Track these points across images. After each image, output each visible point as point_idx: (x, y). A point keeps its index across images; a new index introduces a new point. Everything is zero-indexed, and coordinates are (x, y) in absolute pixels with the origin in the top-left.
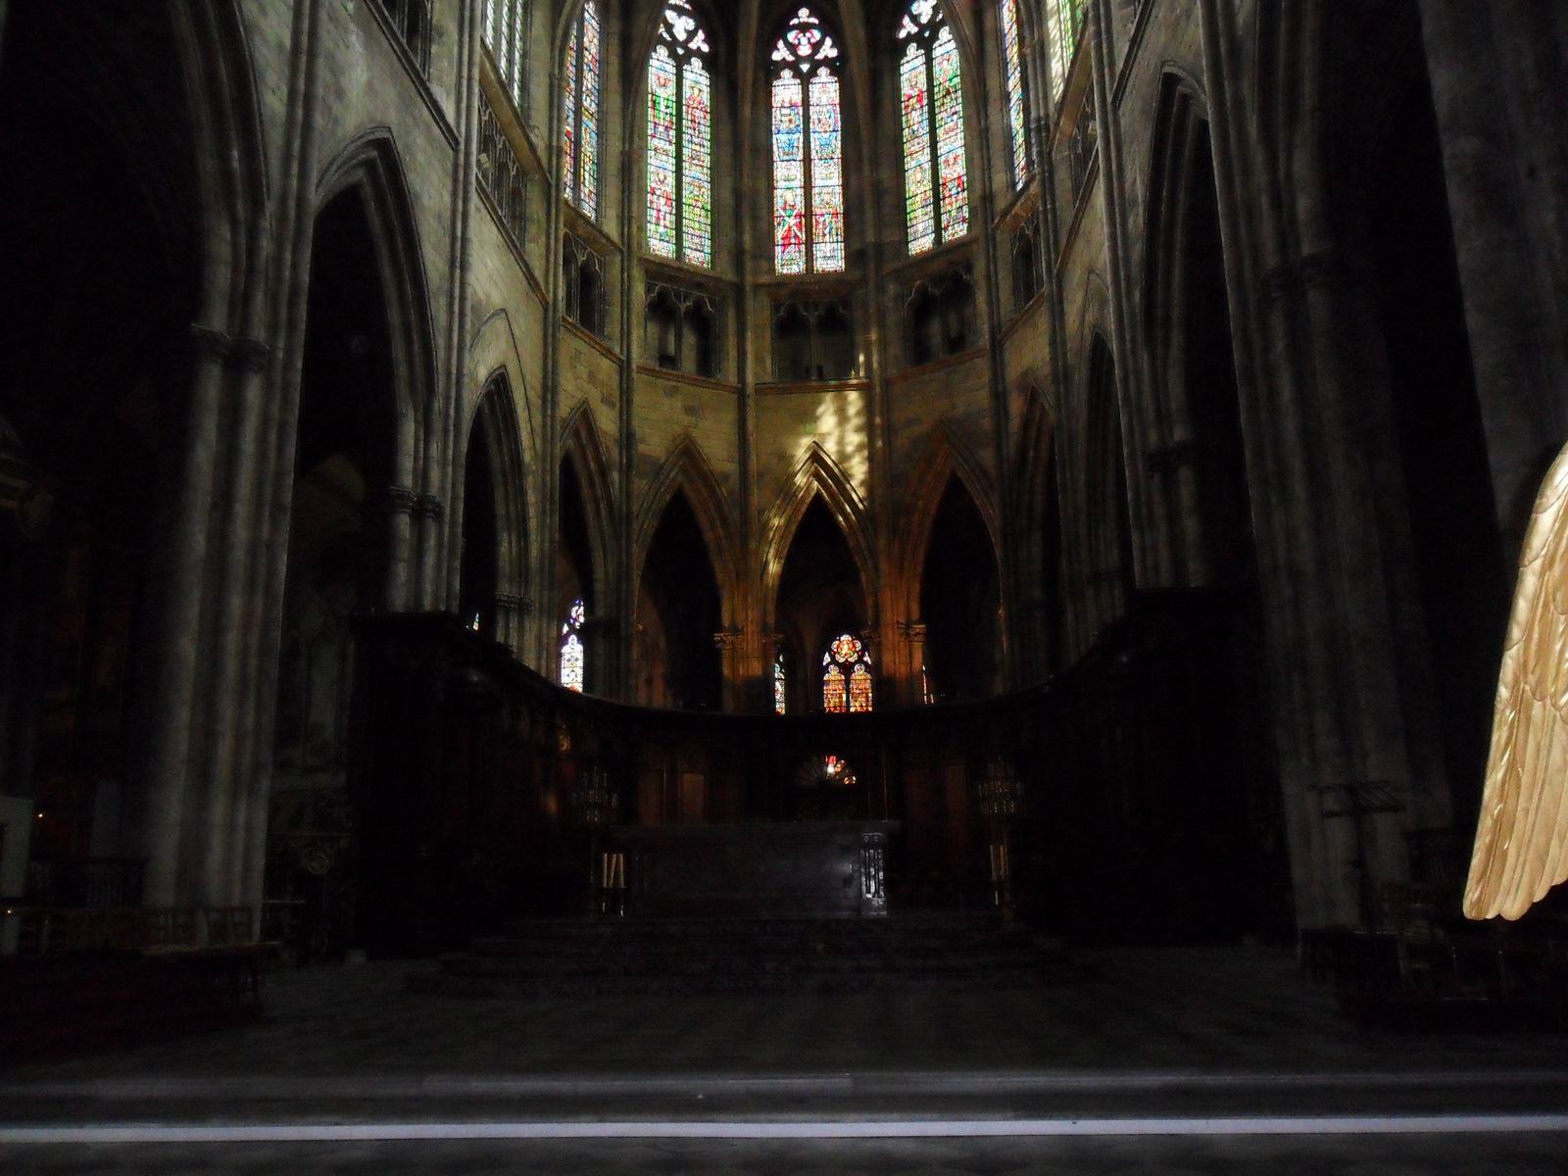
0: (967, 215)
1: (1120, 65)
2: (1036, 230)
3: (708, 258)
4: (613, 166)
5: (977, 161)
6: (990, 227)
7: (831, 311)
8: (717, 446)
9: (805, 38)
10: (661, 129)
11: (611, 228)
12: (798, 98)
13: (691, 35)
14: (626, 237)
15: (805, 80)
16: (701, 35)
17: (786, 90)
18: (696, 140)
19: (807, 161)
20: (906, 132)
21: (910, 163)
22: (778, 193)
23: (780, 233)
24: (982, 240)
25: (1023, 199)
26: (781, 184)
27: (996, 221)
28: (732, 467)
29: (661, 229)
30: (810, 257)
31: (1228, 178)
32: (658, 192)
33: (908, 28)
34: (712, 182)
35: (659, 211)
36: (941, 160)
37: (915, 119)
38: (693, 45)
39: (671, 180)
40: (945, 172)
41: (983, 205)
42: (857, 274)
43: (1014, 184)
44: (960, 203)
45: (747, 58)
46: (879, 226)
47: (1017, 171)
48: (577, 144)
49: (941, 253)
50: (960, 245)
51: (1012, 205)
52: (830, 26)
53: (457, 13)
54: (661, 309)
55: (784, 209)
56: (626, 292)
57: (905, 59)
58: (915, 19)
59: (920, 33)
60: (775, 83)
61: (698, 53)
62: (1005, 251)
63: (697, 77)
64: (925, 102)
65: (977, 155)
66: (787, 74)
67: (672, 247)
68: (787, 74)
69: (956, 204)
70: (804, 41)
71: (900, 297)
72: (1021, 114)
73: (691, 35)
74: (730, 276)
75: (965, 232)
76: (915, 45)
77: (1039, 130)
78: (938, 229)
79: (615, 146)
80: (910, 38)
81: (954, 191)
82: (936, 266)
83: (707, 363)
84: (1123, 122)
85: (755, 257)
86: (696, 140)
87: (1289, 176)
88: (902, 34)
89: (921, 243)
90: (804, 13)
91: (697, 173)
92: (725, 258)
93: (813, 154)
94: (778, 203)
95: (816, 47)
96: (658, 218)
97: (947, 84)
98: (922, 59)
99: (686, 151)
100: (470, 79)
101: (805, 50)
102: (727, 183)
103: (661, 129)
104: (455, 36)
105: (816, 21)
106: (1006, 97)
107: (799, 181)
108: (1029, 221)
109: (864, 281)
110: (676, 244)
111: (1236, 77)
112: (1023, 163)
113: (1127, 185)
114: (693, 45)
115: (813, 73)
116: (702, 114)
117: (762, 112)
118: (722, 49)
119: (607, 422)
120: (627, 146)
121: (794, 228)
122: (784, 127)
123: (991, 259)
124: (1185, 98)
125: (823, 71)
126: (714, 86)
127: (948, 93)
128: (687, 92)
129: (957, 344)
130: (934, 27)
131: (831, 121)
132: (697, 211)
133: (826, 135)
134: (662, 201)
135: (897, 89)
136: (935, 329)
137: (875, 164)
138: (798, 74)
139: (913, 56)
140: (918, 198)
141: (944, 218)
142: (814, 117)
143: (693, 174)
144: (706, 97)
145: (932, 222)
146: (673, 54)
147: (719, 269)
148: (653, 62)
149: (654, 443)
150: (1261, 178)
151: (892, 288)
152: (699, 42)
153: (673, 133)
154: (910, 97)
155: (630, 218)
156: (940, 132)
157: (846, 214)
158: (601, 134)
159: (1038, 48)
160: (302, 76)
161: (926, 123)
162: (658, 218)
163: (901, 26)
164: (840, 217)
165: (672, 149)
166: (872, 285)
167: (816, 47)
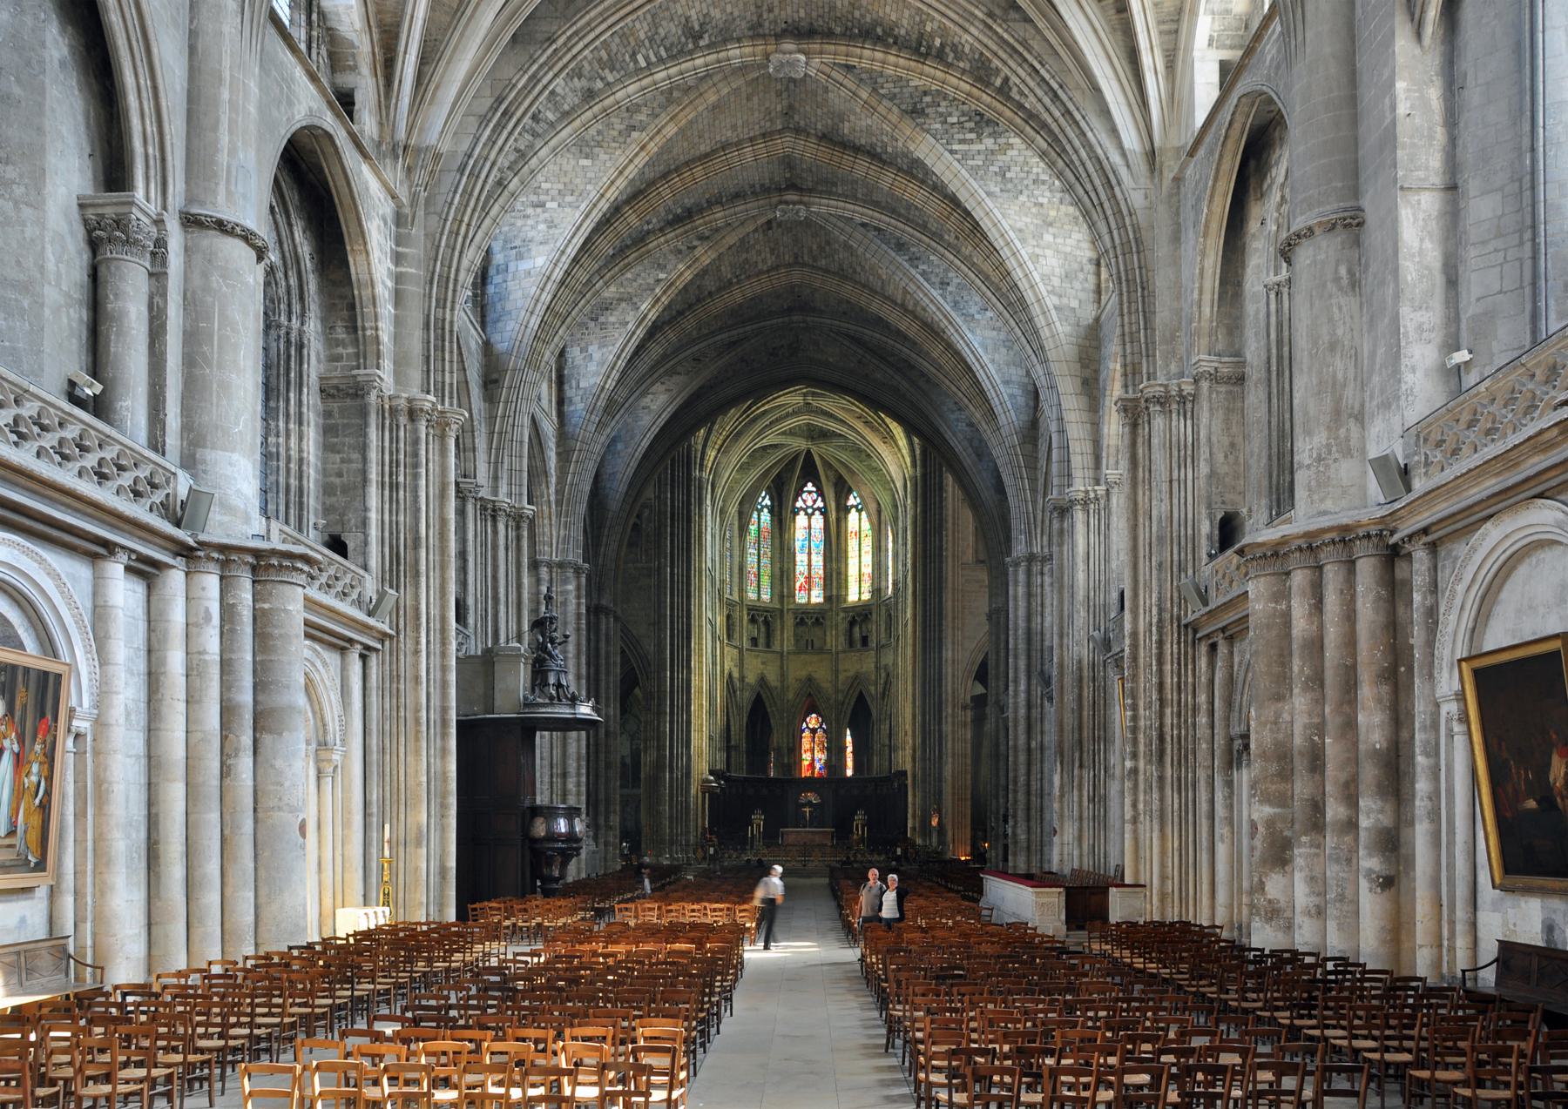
4: (736, 570)
7: (817, 619)
8: (773, 678)
9: (809, 497)
11: (736, 597)
12: (806, 525)
15: (810, 516)
17: (801, 520)
19: (809, 554)
23: (798, 585)
28: (778, 684)
33: (852, 501)
37: (852, 544)
41: (877, 591)
52: (820, 493)
54: (753, 620)
56: (741, 620)
61: (766, 506)
62: (883, 612)
63: (766, 516)
66: (802, 513)
68: (802, 513)
69: (866, 586)
71: (844, 618)
73: (764, 498)
76: (854, 510)
79: (736, 559)
80: (852, 506)
83: (768, 645)
89: (853, 597)
90: (810, 484)
91: (765, 561)
92: (776, 598)
94: (797, 572)
101: (810, 503)
102: (778, 565)
106: (887, 550)
107: (806, 563)
109: (831, 610)
115: (813, 514)
119: (736, 675)
125: (817, 513)
129: (865, 641)
135: (846, 527)
136: (857, 629)
137: (838, 561)
138: (807, 514)
139: (853, 516)
149: (751, 678)
151: (842, 615)
152: (767, 502)
167: (815, 501)
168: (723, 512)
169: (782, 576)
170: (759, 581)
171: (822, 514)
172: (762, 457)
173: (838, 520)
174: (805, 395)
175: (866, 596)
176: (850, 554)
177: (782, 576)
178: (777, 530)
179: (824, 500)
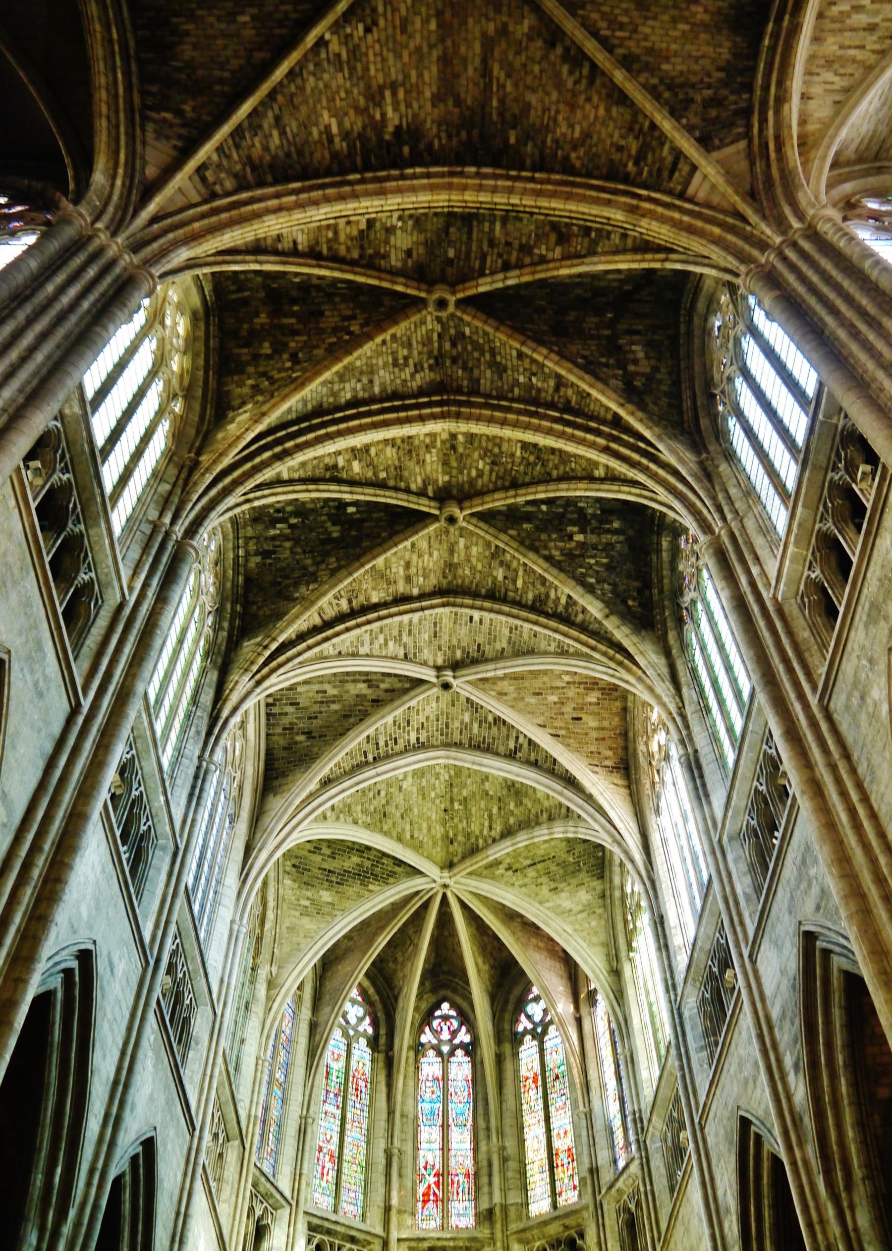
0: (577, 1183)
1: (702, 1099)
2: (638, 1204)
3: (360, 1211)
4: (291, 1130)
5: (584, 1139)
6: (598, 1198)
10: (332, 1095)
12: (439, 1074)
13: (360, 1020)
14: (297, 1191)
15: (445, 1059)
16: (367, 1020)
17: (430, 1066)
18: (358, 1106)
19: (445, 1127)
20: (525, 1107)
21: (529, 1135)
22: (422, 1153)
24: (591, 1208)
25: (625, 1176)
26: (423, 1146)
27: (603, 1191)
29: (324, 1184)
30: (445, 1215)
31: (810, 1225)
32: (325, 1150)
33: (524, 1024)
34: (368, 1143)
35: (323, 1168)
36: (554, 1133)
37: (532, 1097)
38: (361, 1029)
39: (336, 1139)
40: (557, 1144)
42: (485, 1232)
43: (615, 1161)
44: (570, 1172)
45: (404, 1039)
46: (504, 1191)
47: (617, 1149)
48: (266, 1109)
49: (556, 1218)
50: (573, 1212)
51: (616, 1180)
52: (466, 1018)
53: (210, 1024)
55: (425, 1168)
57: (522, 1048)
58: (529, 1017)
59: (534, 1029)
60: (422, 1060)
62: (612, 1221)
63: (362, 1054)
64: (540, 1083)
65: (584, 1133)
66: (431, 1053)
67: (331, 1200)
70: (445, 1028)
72: (617, 1101)
74: (379, 1230)
75: (576, 1198)
76: (528, 1037)
77: (634, 1121)
78: (554, 1194)
80: (526, 1031)
81: (565, 1161)
82: (554, 1230)
84: (710, 1140)
85: (400, 1212)
86: (358, 1106)
87: (856, 1229)
88: (520, 1028)
89: (540, 1206)
93: (451, 1121)
95: (454, 1034)
96: (323, 1174)
97: (556, 1070)
98: (535, 1050)
99: (349, 1116)
100: (211, 1077)
101: (446, 1036)
102: (381, 1145)
103: (332, 1095)
104: (206, 1043)
105: (453, 1013)
106: (603, 1087)
107: (437, 1146)
108: (631, 1197)
109: (493, 1239)
110: (336, 1197)
111: (801, 1144)
112: (621, 1145)
113: (720, 1193)
114: (361, 1029)
115: (452, 1053)
116: (364, 1084)
117: (411, 1083)
118: (383, 1031)
120: (305, 1113)
121: (433, 1186)
122: (427, 1096)
123: (601, 1226)
124: (758, 1137)
125: (459, 1052)
126: (372, 1061)
127: (557, 1077)
128: (354, 1065)
130: (546, 1025)
131: (466, 1093)
132: (355, 1167)
133: (461, 1106)
134: (327, 1158)
135: (517, 1071)
137: (501, 1133)
138: (440, 1054)
139: (528, 1050)
140: (537, 1164)
141: (557, 1183)
142: (451, 1090)
143: (353, 1134)
144: (367, 1070)
145: (548, 1187)
146: (345, 1034)
147: (368, 1222)
148: (332, 1042)
150: (835, 1229)
152: (366, 1026)
153: (340, 1099)
154: (527, 1079)
155: (300, 1175)
156: (552, 1109)
157: (476, 1174)
158: (284, 1101)
159: (628, 1055)
160: (117, 1102)
161: (541, 1101)
162: (323, 1174)
163: (517, 1021)
164: (472, 1177)
165: (338, 1113)
166: (499, 1244)
167: (454, 1034)
168: (271, 984)
169: (389, 1165)
170: (339, 1171)
171: (467, 1053)
172: (360, 896)
173: (499, 1059)
174: (438, 669)
175: (569, 1197)
176: (528, 1120)
177: (389, 1165)
178: (382, 1078)
179: (472, 1029)
